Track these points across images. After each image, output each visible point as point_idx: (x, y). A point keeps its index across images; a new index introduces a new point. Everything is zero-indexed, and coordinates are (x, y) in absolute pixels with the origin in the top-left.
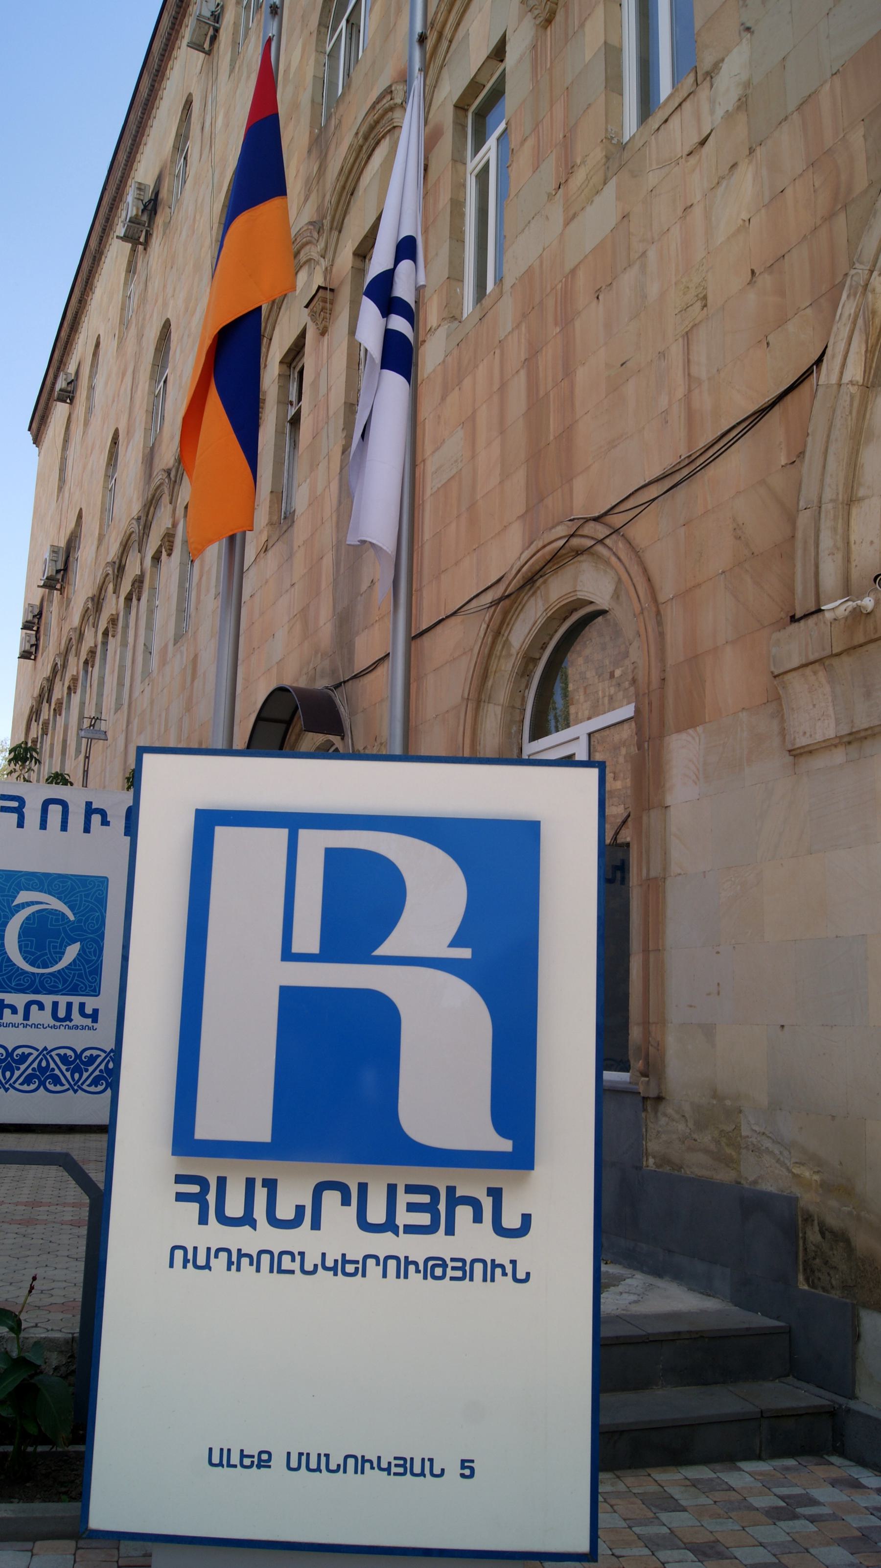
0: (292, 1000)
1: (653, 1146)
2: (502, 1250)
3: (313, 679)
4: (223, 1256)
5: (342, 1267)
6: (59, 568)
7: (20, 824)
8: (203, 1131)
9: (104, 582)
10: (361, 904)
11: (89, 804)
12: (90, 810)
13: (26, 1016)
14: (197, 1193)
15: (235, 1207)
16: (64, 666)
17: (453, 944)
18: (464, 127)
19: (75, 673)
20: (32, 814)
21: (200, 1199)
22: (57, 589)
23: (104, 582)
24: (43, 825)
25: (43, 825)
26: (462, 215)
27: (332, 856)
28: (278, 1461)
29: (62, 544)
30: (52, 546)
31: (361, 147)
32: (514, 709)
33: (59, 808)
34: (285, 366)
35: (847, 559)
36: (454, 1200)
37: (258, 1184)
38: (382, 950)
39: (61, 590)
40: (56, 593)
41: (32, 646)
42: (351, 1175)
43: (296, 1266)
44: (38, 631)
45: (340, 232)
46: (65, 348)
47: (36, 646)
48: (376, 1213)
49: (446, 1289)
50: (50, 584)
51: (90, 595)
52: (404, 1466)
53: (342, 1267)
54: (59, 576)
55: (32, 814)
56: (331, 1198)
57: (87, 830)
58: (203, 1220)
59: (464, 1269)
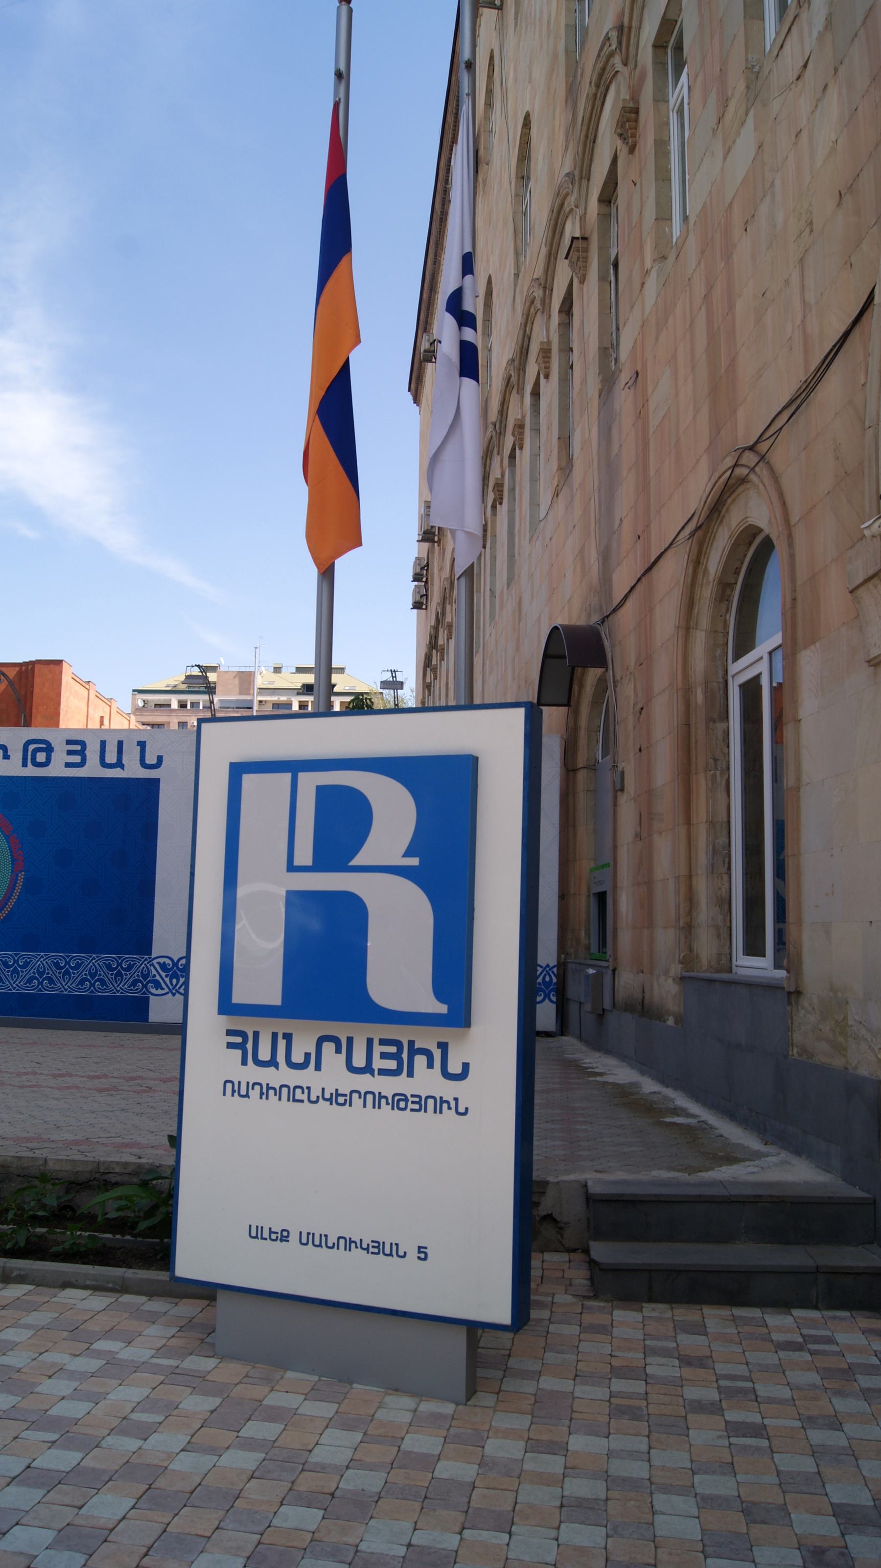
1: (797, 1037)
2: (447, 1089)
3: (589, 616)
4: (257, 1087)
5: (336, 1098)
8: (238, 997)
14: (241, 1043)
15: (264, 1054)
17: (406, 854)
18: (664, 64)
21: (242, 1046)
26: (667, 154)
27: (322, 792)
28: (294, 1237)
31: (595, 95)
32: (716, 633)
34: (564, 315)
36: (414, 1051)
37: (280, 1036)
38: (356, 861)
39: (439, 542)
41: (422, 596)
42: (341, 1030)
43: (305, 1097)
44: (426, 582)
45: (589, 180)
46: (428, 309)
48: (359, 1060)
52: (378, 1248)
53: (336, 1098)
56: (328, 1048)
58: (244, 1062)
59: (420, 1103)
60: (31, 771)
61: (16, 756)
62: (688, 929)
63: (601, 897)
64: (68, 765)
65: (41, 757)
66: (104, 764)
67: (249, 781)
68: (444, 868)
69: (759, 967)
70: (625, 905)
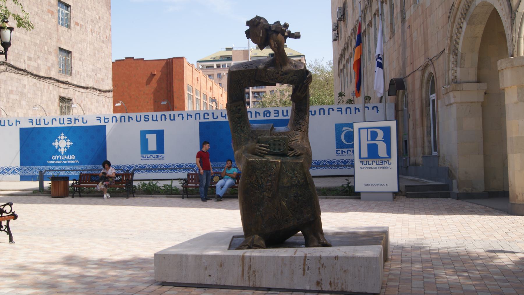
0: (368, 144)
5: (375, 168)
10: (374, 135)
14: (362, 162)
27: (371, 131)
35: (449, 78)
42: (375, 160)
49: (384, 169)
53: (375, 168)
59: (386, 168)
62: (423, 147)
63: (406, 141)
67: (361, 130)
68: (387, 139)
69: (435, 153)
70: (411, 143)
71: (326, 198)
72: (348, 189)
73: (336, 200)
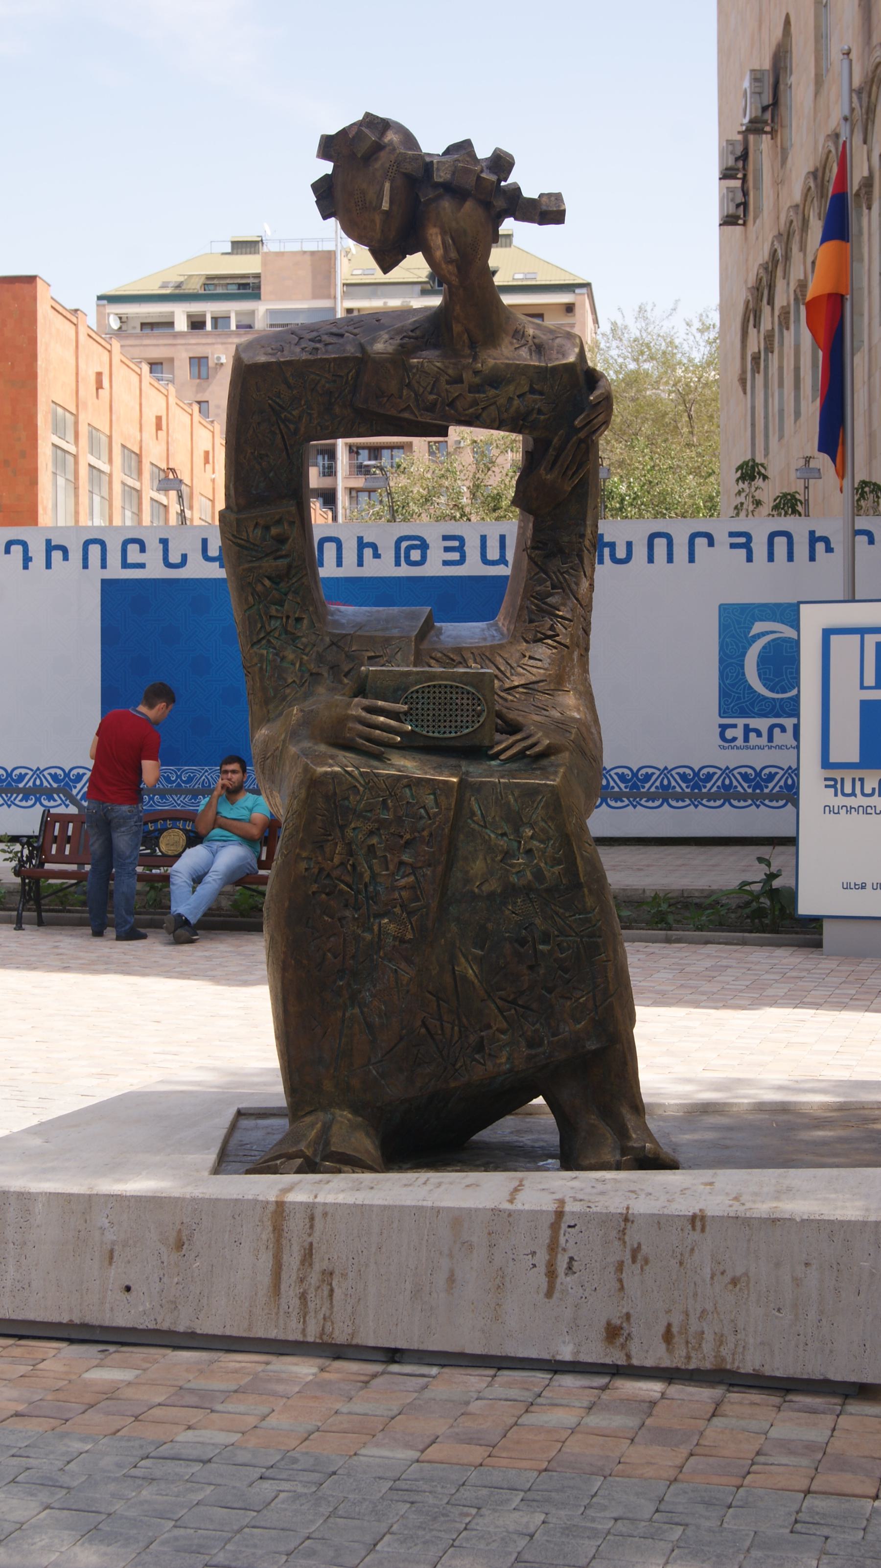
4: (844, 808)
6: (766, 103)
7: (749, 559)
8: (832, 759)
9: (827, 158)
11: (812, 533)
12: (813, 539)
13: (770, 739)
14: (833, 784)
15: (848, 789)
16: (787, 257)
19: (802, 277)
20: (759, 547)
21: (834, 787)
22: (766, 133)
23: (827, 158)
24: (771, 558)
25: (771, 558)
28: (869, 886)
29: (767, 65)
30: (752, 71)
33: (784, 540)
37: (857, 780)
39: (773, 133)
40: (766, 138)
41: (738, 206)
43: (873, 811)
44: (744, 180)
47: (745, 205)
50: (755, 127)
51: (812, 169)
54: (768, 116)
55: (759, 547)
57: (812, 558)
58: (836, 795)
60: (405, 571)
61: (388, 555)
64: (446, 563)
65: (415, 555)
66: (485, 561)
67: (834, 638)
71: (668, 941)
72: (766, 902)
73: (711, 949)
